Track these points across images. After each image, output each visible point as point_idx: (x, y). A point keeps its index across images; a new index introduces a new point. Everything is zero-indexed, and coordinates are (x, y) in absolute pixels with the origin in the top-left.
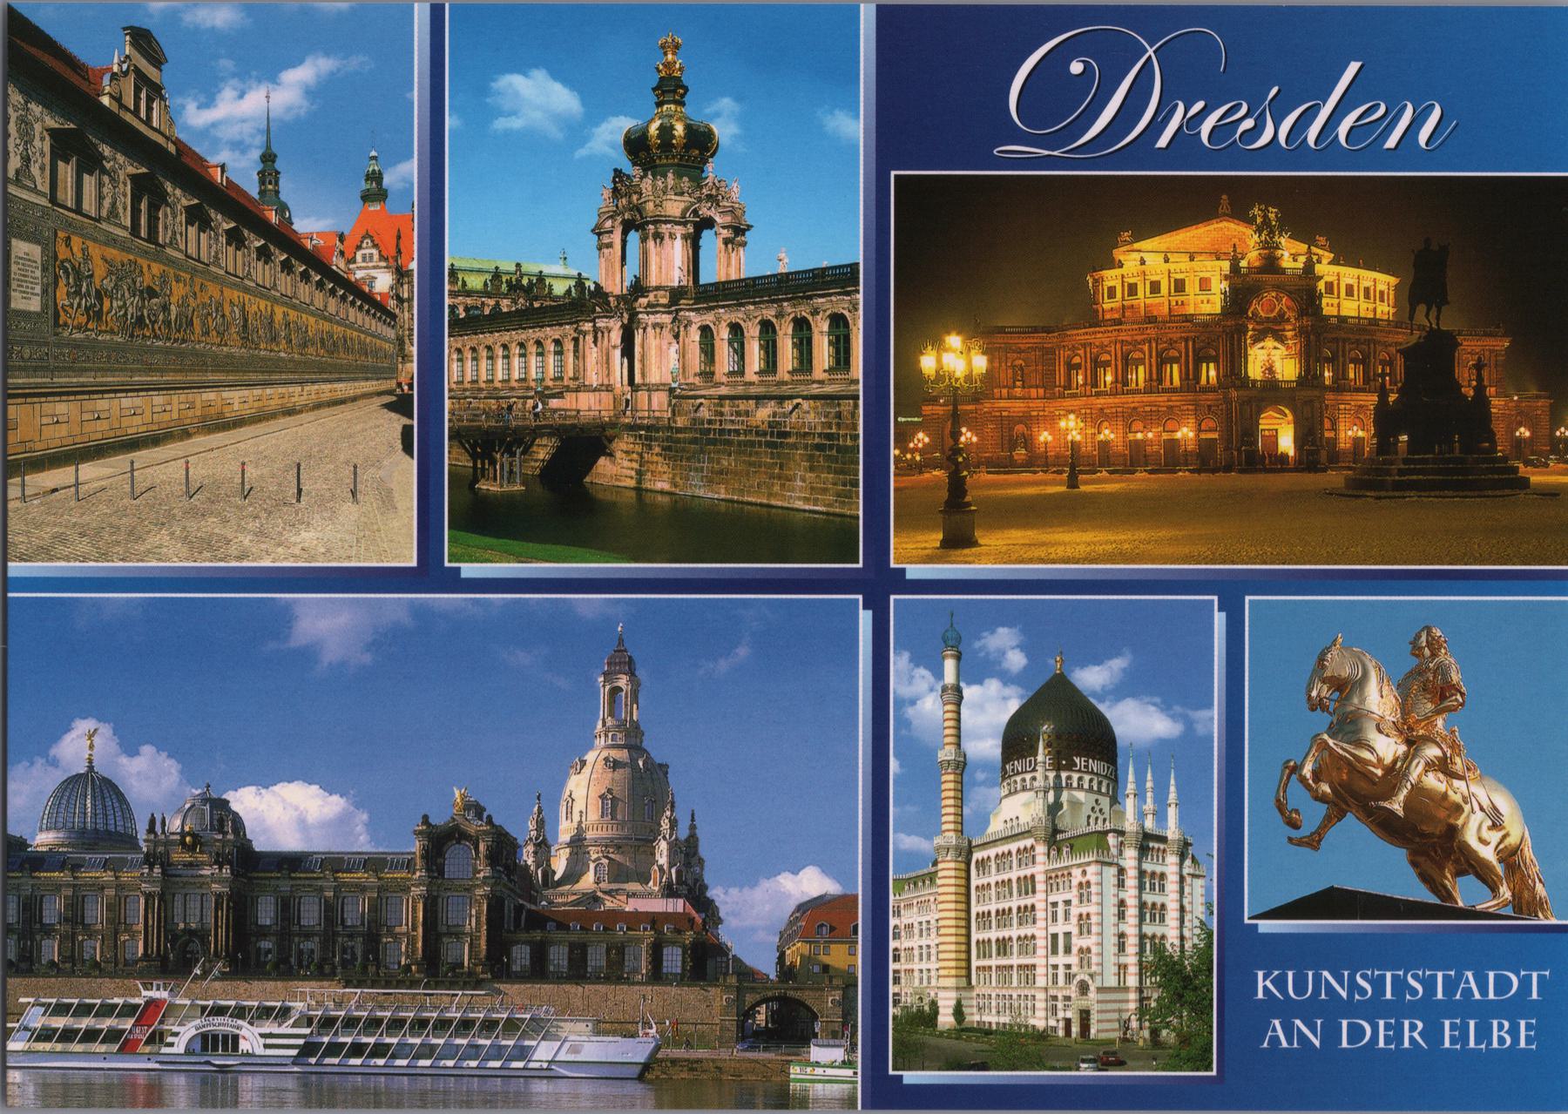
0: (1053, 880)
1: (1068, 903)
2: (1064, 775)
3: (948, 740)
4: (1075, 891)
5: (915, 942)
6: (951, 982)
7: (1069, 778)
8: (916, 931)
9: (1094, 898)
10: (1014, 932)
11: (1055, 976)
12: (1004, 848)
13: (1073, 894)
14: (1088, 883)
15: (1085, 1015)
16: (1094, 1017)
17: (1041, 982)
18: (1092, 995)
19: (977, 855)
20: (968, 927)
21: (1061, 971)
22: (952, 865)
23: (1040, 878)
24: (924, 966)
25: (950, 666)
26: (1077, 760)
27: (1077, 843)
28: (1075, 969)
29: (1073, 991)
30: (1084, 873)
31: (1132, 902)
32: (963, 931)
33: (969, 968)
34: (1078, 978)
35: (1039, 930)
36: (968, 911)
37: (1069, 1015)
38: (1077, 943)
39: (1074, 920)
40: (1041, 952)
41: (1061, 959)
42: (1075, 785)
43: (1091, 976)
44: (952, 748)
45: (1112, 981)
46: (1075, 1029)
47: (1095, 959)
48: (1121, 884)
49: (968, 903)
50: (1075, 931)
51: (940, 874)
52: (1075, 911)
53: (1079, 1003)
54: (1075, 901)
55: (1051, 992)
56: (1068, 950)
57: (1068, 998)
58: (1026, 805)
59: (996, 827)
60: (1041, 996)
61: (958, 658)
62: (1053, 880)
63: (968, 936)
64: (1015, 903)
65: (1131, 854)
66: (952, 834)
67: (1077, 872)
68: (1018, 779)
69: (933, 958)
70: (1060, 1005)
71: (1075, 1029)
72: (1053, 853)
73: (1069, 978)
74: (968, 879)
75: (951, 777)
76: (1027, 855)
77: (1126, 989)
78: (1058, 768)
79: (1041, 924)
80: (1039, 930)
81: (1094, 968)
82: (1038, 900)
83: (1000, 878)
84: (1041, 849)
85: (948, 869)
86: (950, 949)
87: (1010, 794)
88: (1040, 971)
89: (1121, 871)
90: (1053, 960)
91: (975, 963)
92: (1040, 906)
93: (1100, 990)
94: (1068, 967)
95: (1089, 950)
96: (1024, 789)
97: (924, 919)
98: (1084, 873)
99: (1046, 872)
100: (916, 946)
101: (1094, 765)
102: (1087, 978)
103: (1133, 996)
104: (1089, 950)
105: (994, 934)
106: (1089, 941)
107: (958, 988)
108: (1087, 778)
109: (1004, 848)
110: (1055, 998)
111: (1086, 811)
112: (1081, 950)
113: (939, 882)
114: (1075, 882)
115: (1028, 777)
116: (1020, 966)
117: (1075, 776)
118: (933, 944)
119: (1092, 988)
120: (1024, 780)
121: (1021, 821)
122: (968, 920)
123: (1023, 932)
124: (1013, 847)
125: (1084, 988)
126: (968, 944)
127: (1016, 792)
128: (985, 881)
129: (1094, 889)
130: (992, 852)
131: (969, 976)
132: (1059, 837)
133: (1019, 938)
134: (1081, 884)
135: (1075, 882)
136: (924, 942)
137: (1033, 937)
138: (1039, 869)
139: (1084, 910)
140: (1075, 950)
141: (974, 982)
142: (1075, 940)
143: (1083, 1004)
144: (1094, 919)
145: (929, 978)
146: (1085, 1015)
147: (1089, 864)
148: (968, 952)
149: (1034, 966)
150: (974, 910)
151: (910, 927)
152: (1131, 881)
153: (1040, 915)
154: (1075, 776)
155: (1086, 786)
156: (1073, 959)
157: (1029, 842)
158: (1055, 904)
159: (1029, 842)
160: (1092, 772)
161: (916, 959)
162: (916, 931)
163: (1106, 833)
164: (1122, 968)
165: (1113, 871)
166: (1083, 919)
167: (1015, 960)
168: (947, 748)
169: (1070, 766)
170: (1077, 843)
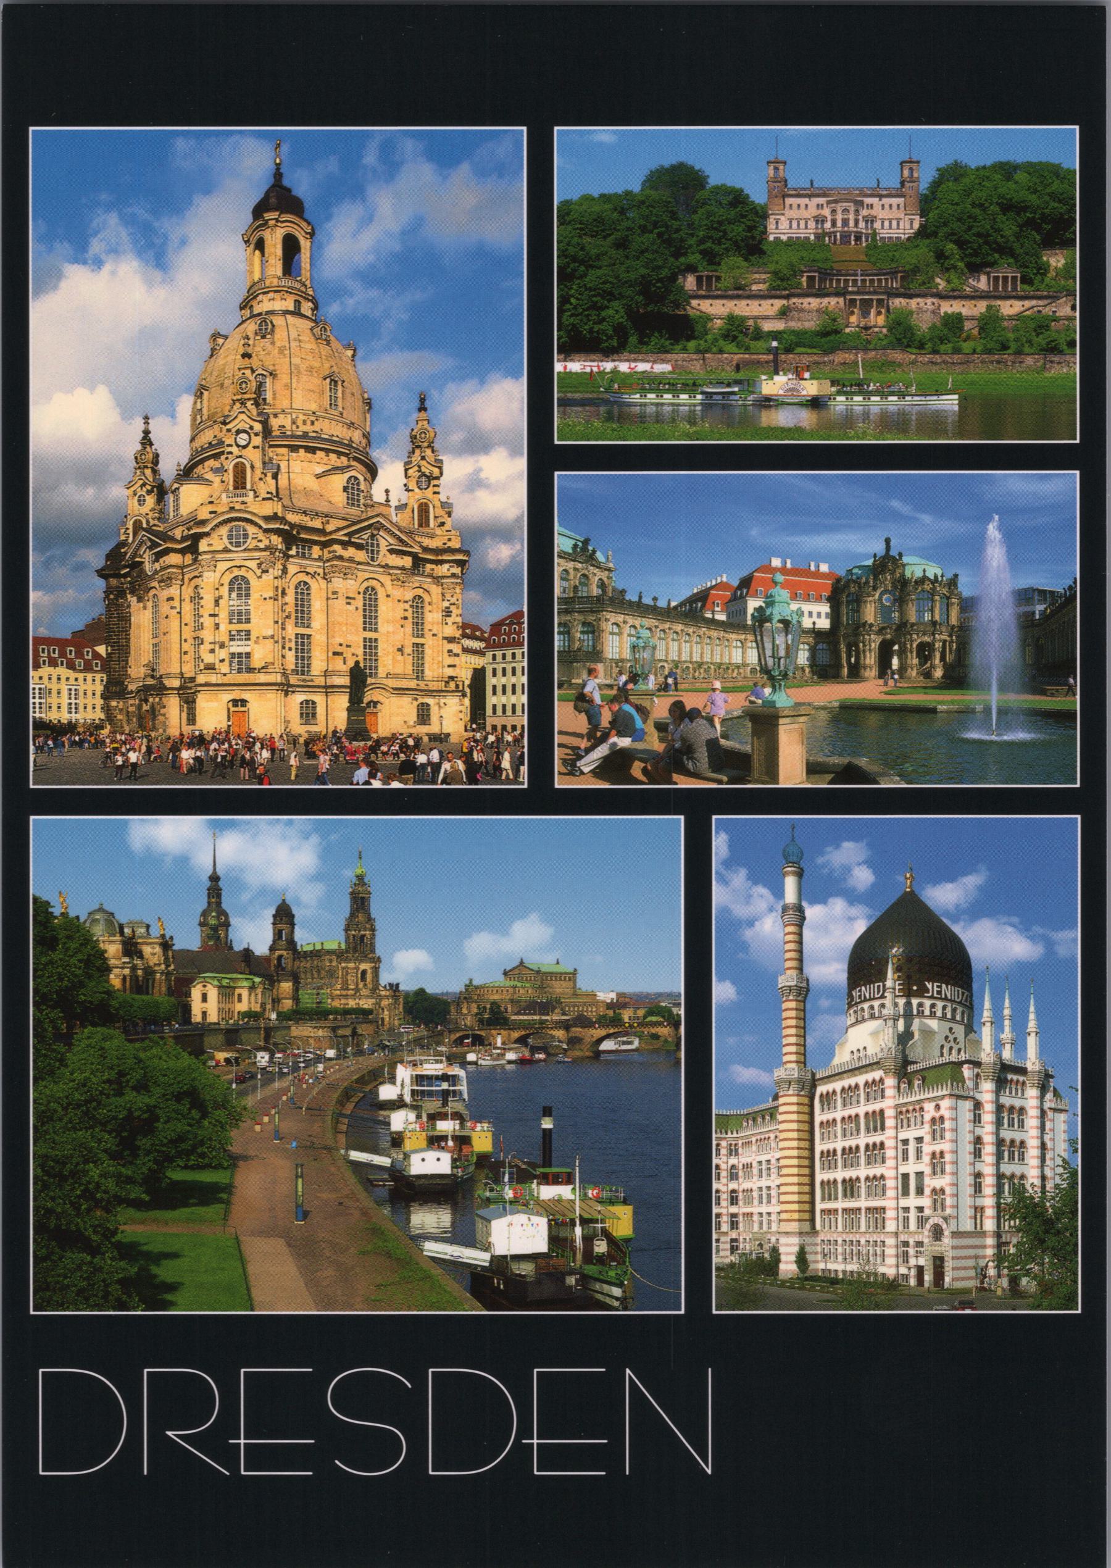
0: (904, 1115)
1: (919, 1140)
2: (915, 1002)
3: (789, 964)
4: (927, 1127)
5: (754, 1184)
6: (794, 1227)
7: (920, 1005)
8: (755, 1171)
9: (948, 1135)
10: (862, 1172)
11: (906, 1220)
12: (851, 1081)
13: (925, 1131)
14: (942, 1118)
15: (939, 1263)
16: (949, 1265)
17: (891, 1226)
18: (947, 1240)
19: (821, 1089)
20: (812, 1167)
21: (913, 1215)
22: (794, 1099)
23: (890, 1113)
24: (764, 1209)
25: (790, 884)
26: (929, 986)
27: (930, 1075)
28: (927, 1212)
29: (925, 1236)
30: (938, 1107)
31: (989, 1139)
32: (806, 1171)
33: (812, 1212)
34: (931, 1222)
35: (888, 1170)
36: (812, 1149)
37: (922, 1262)
38: (930, 1183)
39: (926, 1159)
40: (891, 1193)
41: (912, 1201)
42: (927, 1012)
43: (946, 1219)
44: (793, 973)
45: (968, 1225)
46: (928, 1278)
47: (949, 1201)
48: (977, 1120)
49: (812, 1140)
50: (927, 1170)
51: (781, 1109)
52: (927, 1149)
53: (932, 1248)
54: (927, 1138)
55: (902, 1238)
56: (920, 1191)
57: (920, 1244)
58: (875, 1034)
59: (842, 1057)
60: (891, 1241)
61: (800, 874)
62: (904, 1115)
63: (812, 1176)
64: (862, 1140)
65: (987, 1087)
66: (794, 1065)
67: (929, 1107)
68: (866, 1006)
69: (774, 1201)
70: (911, 1251)
71: (928, 1278)
72: (903, 1086)
73: (922, 1221)
74: (811, 1114)
75: (793, 1005)
76: (875, 1089)
77: (983, 1234)
78: (908, 994)
79: (890, 1163)
80: (888, 1170)
81: (948, 1211)
82: (888, 1137)
83: (846, 1113)
84: (890, 1082)
85: (789, 1103)
86: (792, 1192)
87: (857, 1022)
88: (890, 1214)
89: (978, 1105)
90: (903, 1203)
91: (819, 1206)
92: (890, 1143)
93: (956, 1234)
94: (920, 1209)
95: (942, 1191)
96: (872, 1017)
97: (763, 1158)
98: (938, 1107)
99: (897, 1106)
100: (755, 1188)
101: (947, 990)
102: (941, 1221)
103: (990, 1241)
104: (942, 1191)
105: (840, 1174)
106: (943, 1182)
107: (800, 1234)
108: (940, 1004)
109: (851, 1081)
110: (906, 1244)
111: (939, 1040)
112: (934, 1191)
113: (780, 1118)
114: (927, 1117)
115: (876, 1004)
116: (868, 1209)
117: (928, 1003)
118: (773, 1185)
119: (946, 1233)
120: (872, 1007)
122: (812, 1158)
123: (872, 1172)
124: (861, 1079)
125: (937, 1233)
126: (812, 1185)
127: (864, 1020)
128: (829, 1116)
129: (947, 1125)
130: (837, 1085)
131: (812, 1220)
132: (911, 1068)
133: (867, 1178)
134: (933, 1120)
135: (927, 1117)
136: (764, 1183)
137: (882, 1177)
138: (888, 1104)
139: (937, 1148)
140: (927, 1191)
141: (818, 1227)
142: (927, 1181)
144: (948, 1157)
145: (769, 1223)
146: (939, 1263)
147: (942, 1097)
148: (812, 1193)
149: (884, 1209)
150: (819, 1147)
151: (749, 1166)
152: (988, 1117)
153: (890, 1153)
154: (928, 1003)
155: (939, 1014)
156: (926, 1202)
157: (877, 1074)
158: (905, 1142)
159: (877, 1074)
160: (946, 999)
161: (756, 1202)
162: (755, 1171)
164: (979, 1210)
165: (968, 1105)
166: (937, 1159)
167: (863, 1203)
168: (789, 972)
169: (922, 992)
170: (930, 1075)
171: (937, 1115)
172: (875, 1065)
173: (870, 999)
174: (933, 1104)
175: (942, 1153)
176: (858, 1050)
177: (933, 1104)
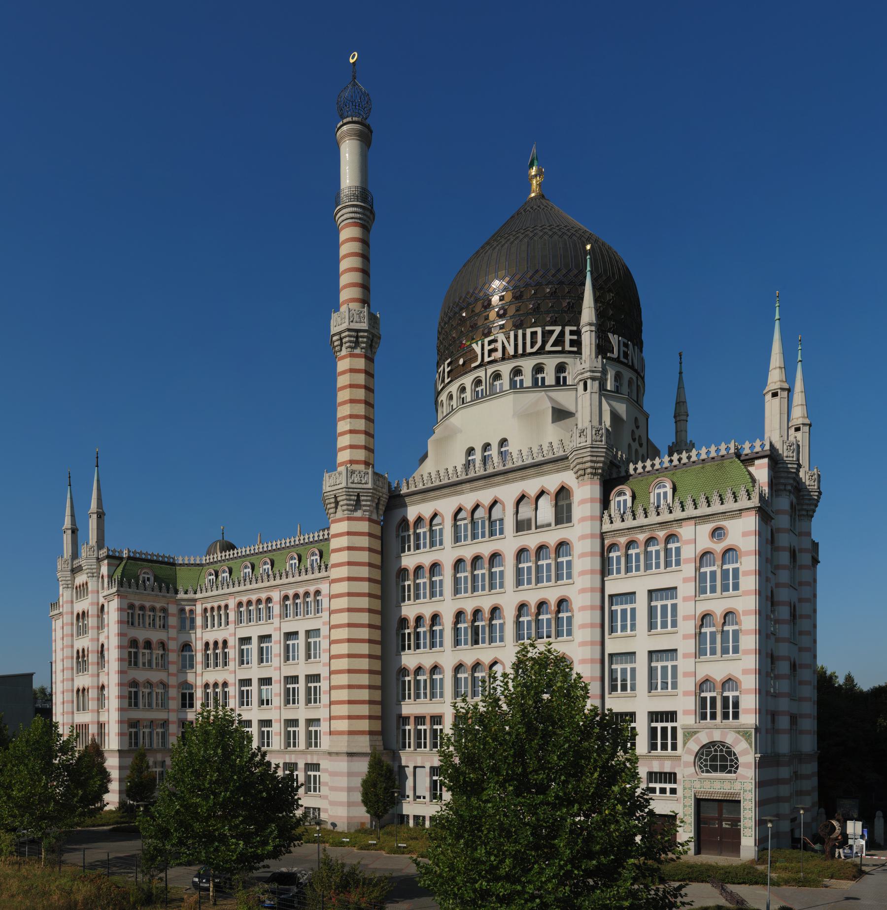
4: (689, 569)
13: (681, 577)
14: (730, 552)
22: (364, 527)
25: (349, 153)
30: (717, 533)
39: (687, 627)
52: (687, 608)
54: (686, 589)
61: (365, 138)
67: (695, 538)
68: (505, 369)
84: (585, 494)
98: (717, 533)
112: (704, 684)
113: (335, 558)
114: (688, 553)
115: (527, 365)
120: (517, 371)
121: (512, 448)
130: (446, 506)
134: (705, 556)
135: (688, 553)
139: (717, 606)
142: (684, 664)
143: (717, 784)
163: (749, 461)
171: (718, 547)
172: (559, 462)
173: (515, 356)
174: (706, 528)
175: (728, 615)
176: (487, 446)
177: (706, 528)
